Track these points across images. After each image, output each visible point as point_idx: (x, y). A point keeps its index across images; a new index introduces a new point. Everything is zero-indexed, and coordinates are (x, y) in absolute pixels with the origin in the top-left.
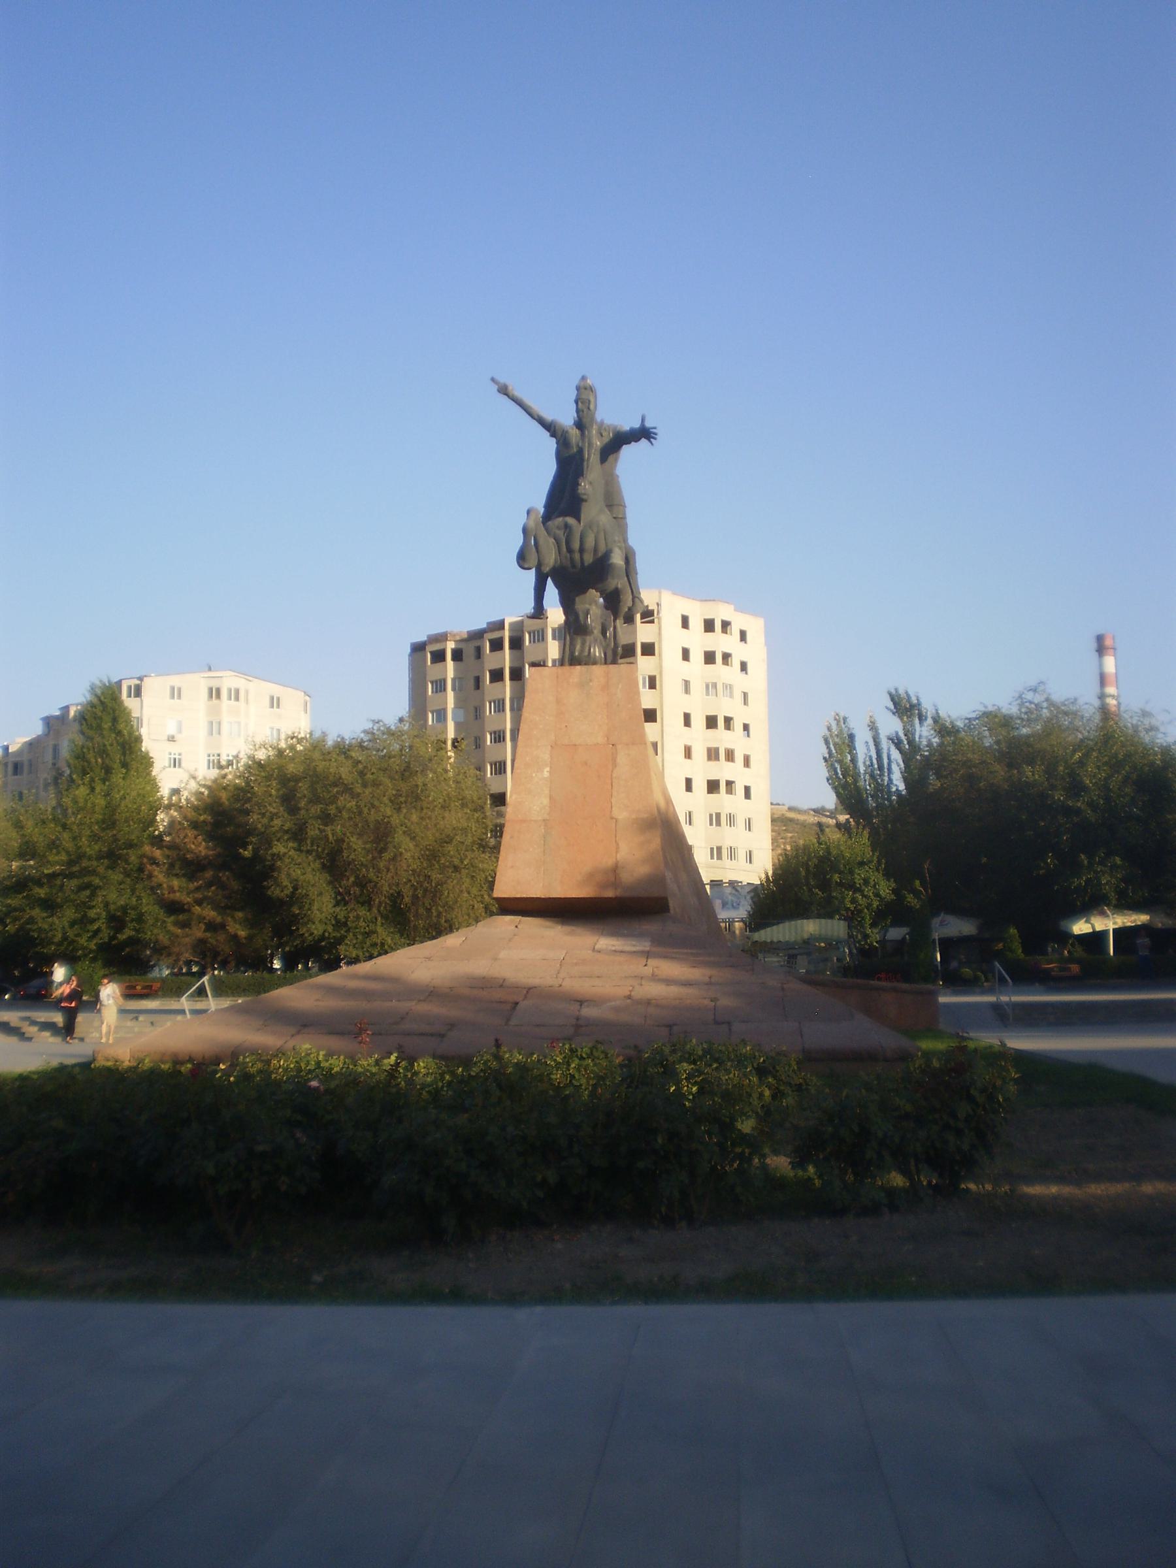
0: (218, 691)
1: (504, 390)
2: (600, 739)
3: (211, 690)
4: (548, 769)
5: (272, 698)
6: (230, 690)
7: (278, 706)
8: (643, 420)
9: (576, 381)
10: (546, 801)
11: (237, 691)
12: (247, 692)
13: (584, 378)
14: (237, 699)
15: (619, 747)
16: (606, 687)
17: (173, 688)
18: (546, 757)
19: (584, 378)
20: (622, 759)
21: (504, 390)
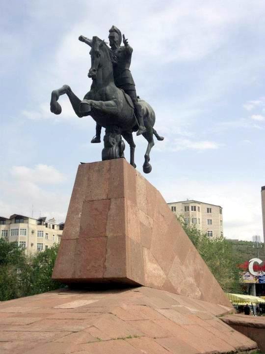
0: (188, 207)
1: (82, 39)
2: (104, 197)
3: (185, 207)
4: (81, 213)
5: (208, 209)
6: (192, 207)
7: (211, 212)
8: (123, 35)
9: (110, 28)
10: (78, 229)
11: (195, 207)
12: (199, 207)
13: (113, 27)
14: (195, 210)
15: (112, 200)
16: (109, 170)
17: (172, 207)
18: (81, 207)
20: (113, 206)
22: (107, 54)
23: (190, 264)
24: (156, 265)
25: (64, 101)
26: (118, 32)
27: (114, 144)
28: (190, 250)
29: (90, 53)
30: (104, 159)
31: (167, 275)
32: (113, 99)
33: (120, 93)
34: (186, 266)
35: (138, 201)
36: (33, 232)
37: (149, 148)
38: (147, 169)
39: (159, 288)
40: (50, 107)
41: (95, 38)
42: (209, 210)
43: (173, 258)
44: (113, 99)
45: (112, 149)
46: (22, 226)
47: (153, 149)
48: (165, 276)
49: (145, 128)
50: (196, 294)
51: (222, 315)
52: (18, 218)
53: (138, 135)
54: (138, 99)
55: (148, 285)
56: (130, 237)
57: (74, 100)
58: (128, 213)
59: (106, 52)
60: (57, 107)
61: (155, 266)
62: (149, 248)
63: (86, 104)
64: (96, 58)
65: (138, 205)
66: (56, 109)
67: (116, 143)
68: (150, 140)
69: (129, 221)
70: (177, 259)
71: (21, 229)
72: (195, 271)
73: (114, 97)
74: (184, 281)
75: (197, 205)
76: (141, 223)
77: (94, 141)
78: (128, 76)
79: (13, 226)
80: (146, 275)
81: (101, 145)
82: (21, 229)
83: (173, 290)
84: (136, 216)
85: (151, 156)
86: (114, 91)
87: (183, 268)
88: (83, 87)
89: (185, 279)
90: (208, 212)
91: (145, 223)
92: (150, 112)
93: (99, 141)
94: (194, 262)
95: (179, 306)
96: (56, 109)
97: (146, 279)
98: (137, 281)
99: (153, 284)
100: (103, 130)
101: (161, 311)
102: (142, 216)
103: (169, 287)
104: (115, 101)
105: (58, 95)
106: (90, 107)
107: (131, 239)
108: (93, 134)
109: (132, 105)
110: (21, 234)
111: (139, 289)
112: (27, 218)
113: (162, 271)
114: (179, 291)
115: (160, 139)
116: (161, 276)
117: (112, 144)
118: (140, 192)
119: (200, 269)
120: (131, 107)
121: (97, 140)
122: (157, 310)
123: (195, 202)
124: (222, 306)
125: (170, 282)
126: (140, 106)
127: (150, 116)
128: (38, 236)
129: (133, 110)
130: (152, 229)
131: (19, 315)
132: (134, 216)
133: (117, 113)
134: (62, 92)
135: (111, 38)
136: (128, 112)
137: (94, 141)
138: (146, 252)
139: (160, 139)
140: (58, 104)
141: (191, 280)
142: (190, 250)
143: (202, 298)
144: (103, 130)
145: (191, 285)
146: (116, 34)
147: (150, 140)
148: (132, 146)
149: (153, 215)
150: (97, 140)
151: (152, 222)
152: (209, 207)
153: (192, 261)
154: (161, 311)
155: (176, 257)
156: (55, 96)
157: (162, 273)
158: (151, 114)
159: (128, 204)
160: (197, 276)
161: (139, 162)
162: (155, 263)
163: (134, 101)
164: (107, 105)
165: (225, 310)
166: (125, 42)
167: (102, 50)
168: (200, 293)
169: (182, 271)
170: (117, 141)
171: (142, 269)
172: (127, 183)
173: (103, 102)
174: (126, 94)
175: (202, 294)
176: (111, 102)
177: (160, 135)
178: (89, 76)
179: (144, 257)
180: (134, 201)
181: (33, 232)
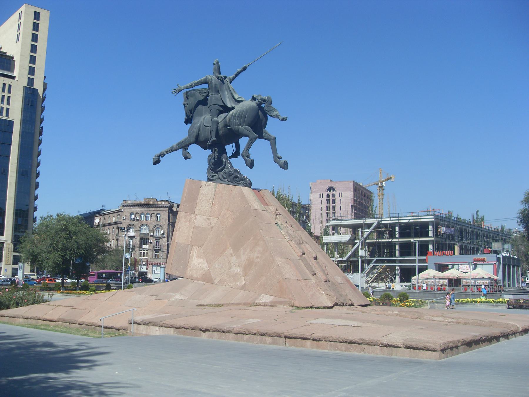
23: (244, 254)
31: (209, 267)
35: (197, 208)
50: (238, 283)
61: (202, 260)
69: (180, 228)
70: (230, 250)
80: (189, 269)
84: (190, 222)
99: (192, 276)
114: (216, 281)
116: (203, 269)
125: (210, 274)
130: (212, 227)
141: (239, 270)
143: (243, 288)
149: (220, 214)
153: (248, 250)
157: (205, 266)
162: (203, 258)
167: (192, 96)
168: (244, 282)
169: (230, 262)
175: (245, 284)
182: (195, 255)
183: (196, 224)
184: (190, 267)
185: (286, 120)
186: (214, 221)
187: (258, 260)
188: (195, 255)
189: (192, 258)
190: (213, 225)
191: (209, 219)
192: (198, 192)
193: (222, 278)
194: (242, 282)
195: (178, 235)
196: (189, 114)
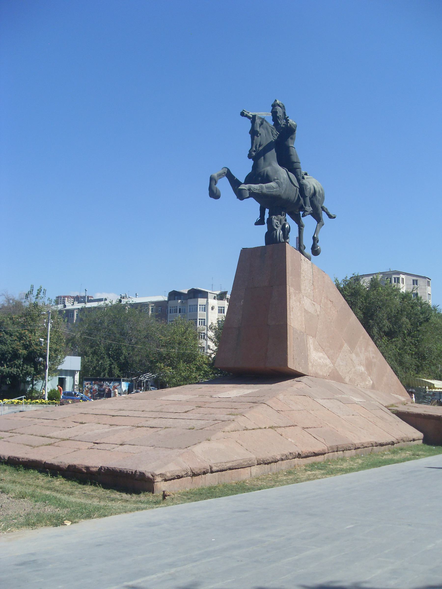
1: (242, 114)
4: (243, 301)
5: (413, 280)
6: (395, 278)
7: (417, 284)
9: (272, 103)
11: (398, 279)
19: (276, 101)
21: (242, 114)
22: (268, 132)
23: (361, 352)
24: (321, 354)
25: (224, 186)
26: (283, 108)
27: (277, 226)
28: (362, 337)
29: (250, 133)
30: (266, 243)
31: (334, 364)
32: (274, 180)
33: (283, 173)
34: (357, 355)
35: (302, 287)
36: (212, 308)
37: (318, 228)
38: (315, 252)
39: (324, 377)
40: (208, 192)
41: (254, 117)
42: (415, 282)
43: (341, 347)
44: (274, 180)
45: (275, 232)
46: (201, 301)
47: (323, 230)
48: (331, 365)
49: (311, 209)
50: (367, 383)
51: (392, 405)
52: (196, 294)
53: (304, 216)
54: (305, 176)
55: (312, 375)
56: (292, 325)
57: (235, 183)
58: (291, 301)
59: (267, 129)
60: (215, 191)
61: (321, 354)
62: (314, 336)
63: (244, 189)
64: (256, 137)
65: (303, 291)
66: (214, 194)
67: (280, 226)
68: (318, 219)
69: (293, 308)
70: (346, 347)
71: (200, 305)
72: (367, 359)
73: (276, 178)
74: (353, 370)
75: (402, 276)
76: (306, 311)
77: (257, 223)
78: (292, 153)
79: (191, 302)
81: (264, 228)
82: (200, 305)
83: (339, 379)
84: (300, 303)
85: (320, 236)
86: (276, 172)
87: (353, 356)
88: (242, 169)
89: (354, 367)
90: (414, 284)
91: (311, 310)
92: (317, 190)
93: (263, 224)
94: (366, 350)
95: (343, 396)
96: (214, 194)
97: (310, 368)
98: (300, 370)
99: (317, 373)
100: (267, 211)
101: (320, 401)
102: (307, 303)
103: (336, 377)
104: (277, 183)
105: (216, 178)
106: (248, 192)
107: (293, 328)
108: (257, 216)
109: (297, 185)
110: (200, 311)
111: (301, 378)
112: (207, 293)
113: (328, 360)
114: (347, 380)
115: (330, 217)
117: (276, 228)
118: (306, 277)
119: (373, 357)
120: (296, 187)
121: (260, 222)
122: (317, 400)
123: (399, 273)
124: (396, 396)
126: (306, 186)
127: (317, 195)
128: (219, 313)
129: (298, 189)
130: (318, 316)
131: (179, 402)
132: (298, 304)
133: (279, 195)
134: (220, 176)
135: (274, 113)
136: (292, 193)
137: (257, 223)
138: (311, 340)
139: (330, 217)
140: (216, 188)
142: (362, 337)
143: (373, 387)
144: (267, 211)
145: (362, 374)
146: (279, 109)
147: (318, 219)
148: (301, 227)
149: (321, 301)
150: (260, 222)
151: (318, 309)
152: (415, 278)
153: (363, 349)
154: (320, 401)
155: (346, 345)
156: (213, 180)
157: (328, 361)
158: (319, 192)
159: (291, 291)
160: (369, 365)
161: (308, 243)
162: (321, 352)
163: (298, 180)
164: (267, 188)
165: (398, 399)
166: (287, 120)
167: (263, 128)
168: (371, 382)
169: (352, 360)
170: (280, 224)
171: (306, 358)
172: (290, 269)
173: (264, 185)
174: (289, 173)
176: (272, 184)
177: (331, 213)
178: (250, 156)
179: (308, 346)
180: (298, 288)
181: (212, 308)
182: (312, 346)
183: (305, 307)
184: (311, 362)
185: (335, 218)
186: (318, 308)
187: (375, 360)
188: (312, 346)
189: (310, 350)
190: (318, 313)
191: (314, 305)
192: (300, 266)
193: (351, 377)
194: (369, 381)
195: (292, 317)
196: (258, 147)
